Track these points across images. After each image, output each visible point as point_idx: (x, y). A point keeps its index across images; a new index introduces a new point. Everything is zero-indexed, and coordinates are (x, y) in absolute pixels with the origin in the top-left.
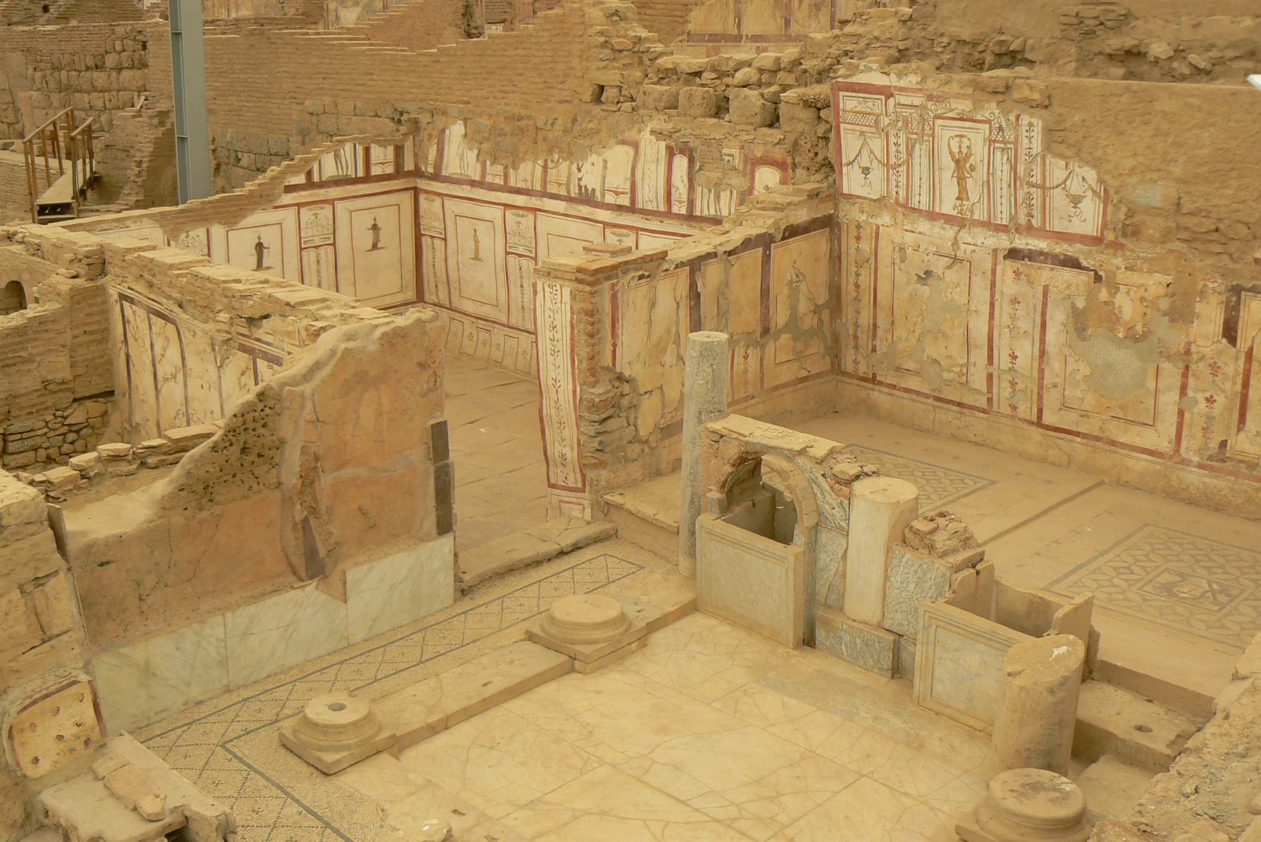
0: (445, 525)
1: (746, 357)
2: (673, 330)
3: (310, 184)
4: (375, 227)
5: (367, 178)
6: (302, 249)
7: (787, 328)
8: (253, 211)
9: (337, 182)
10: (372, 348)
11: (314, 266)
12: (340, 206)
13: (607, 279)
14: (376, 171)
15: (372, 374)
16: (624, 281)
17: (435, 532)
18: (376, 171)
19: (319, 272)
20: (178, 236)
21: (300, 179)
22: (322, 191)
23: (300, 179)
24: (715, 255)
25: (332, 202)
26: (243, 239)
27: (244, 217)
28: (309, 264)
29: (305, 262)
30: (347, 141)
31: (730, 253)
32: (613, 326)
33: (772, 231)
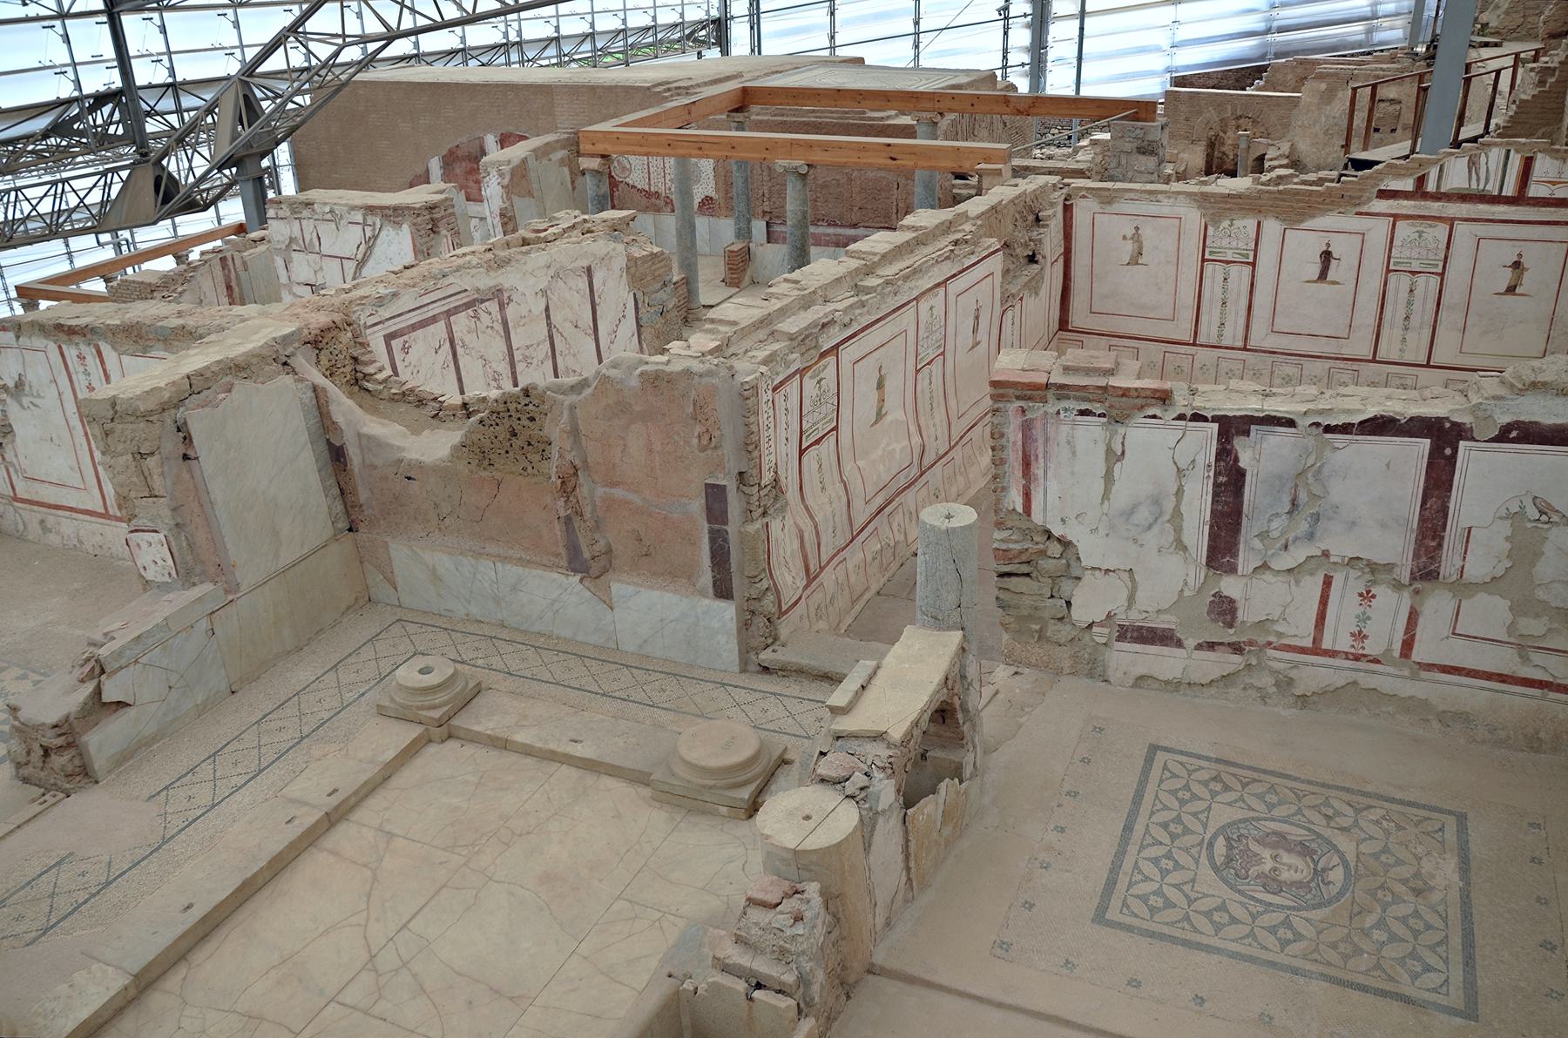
0: (723, 590)
1: (1367, 596)
2: (1169, 505)
3: (1420, 192)
4: (1517, 265)
5: (1520, 199)
6: (1388, 271)
7: (1491, 585)
8: (1324, 212)
9: (1464, 197)
10: (634, 382)
11: (1404, 294)
12: (1460, 228)
13: (1018, 398)
14: (1534, 191)
15: (637, 408)
16: (1051, 407)
17: (711, 590)
18: (1534, 191)
19: (1410, 303)
20: (1220, 222)
21: (1408, 185)
22: (1437, 204)
23: (1408, 185)
24: (1291, 423)
25: (1451, 222)
26: (1304, 244)
27: (1313, 216)
28: (1397, 290)
29: (1391, 286)
30: (1496, 144)
31: (1329, 429)
32: (1027, 464)
33: (1466, 419)
